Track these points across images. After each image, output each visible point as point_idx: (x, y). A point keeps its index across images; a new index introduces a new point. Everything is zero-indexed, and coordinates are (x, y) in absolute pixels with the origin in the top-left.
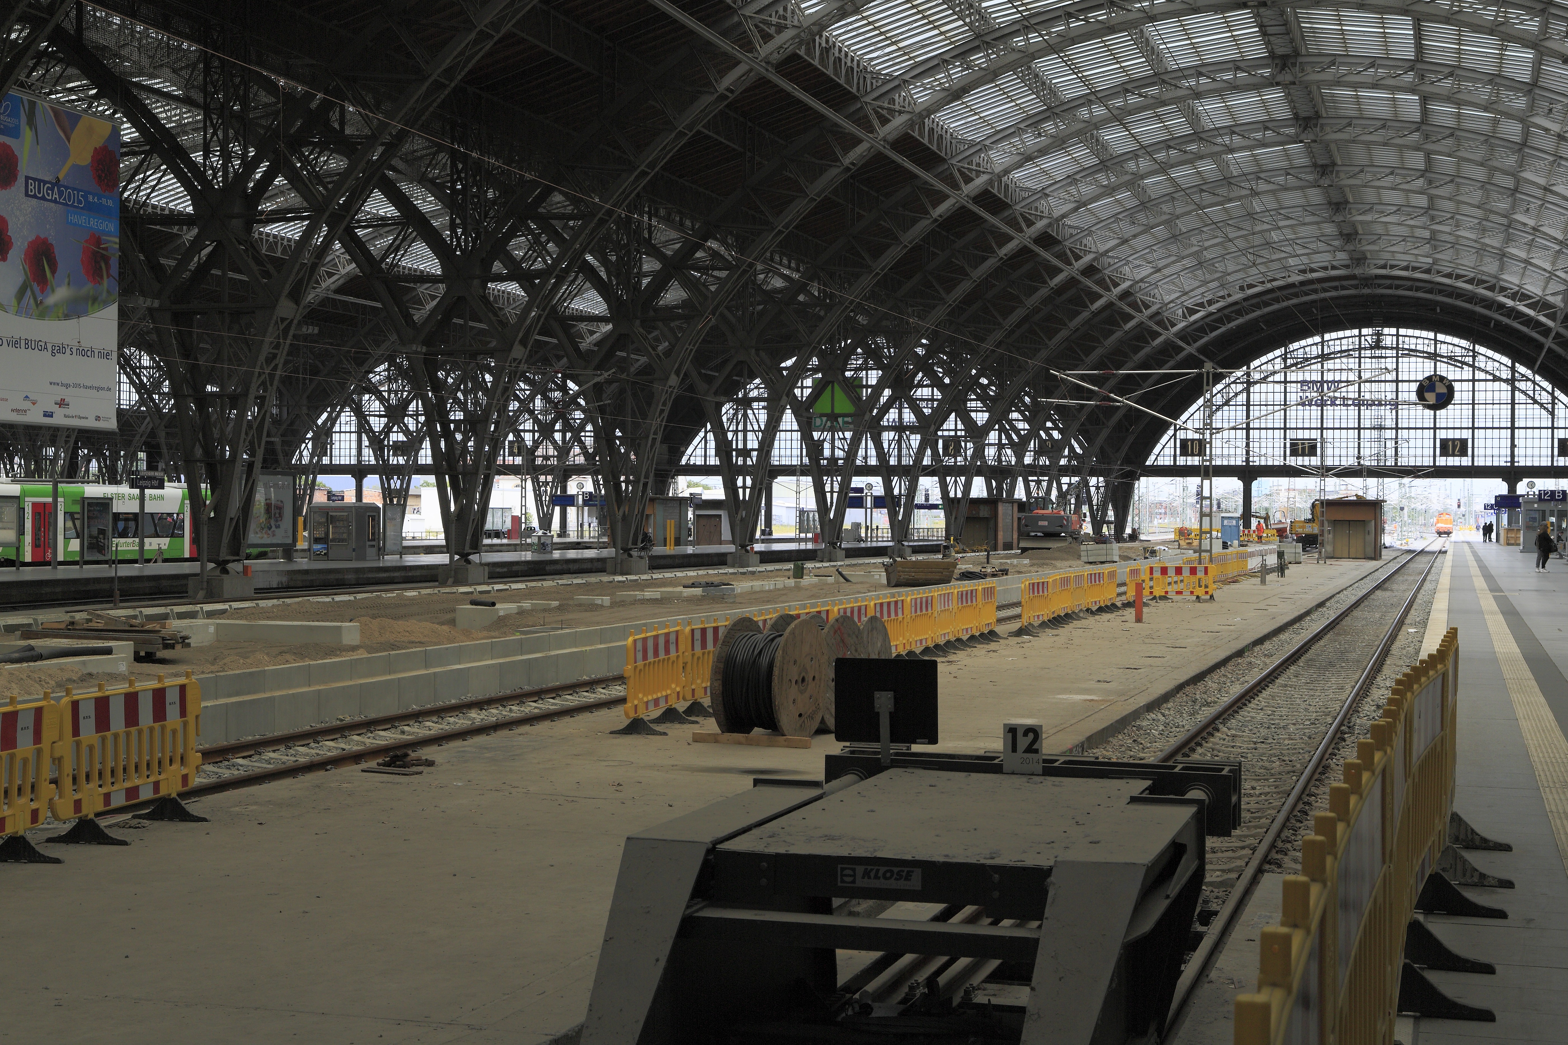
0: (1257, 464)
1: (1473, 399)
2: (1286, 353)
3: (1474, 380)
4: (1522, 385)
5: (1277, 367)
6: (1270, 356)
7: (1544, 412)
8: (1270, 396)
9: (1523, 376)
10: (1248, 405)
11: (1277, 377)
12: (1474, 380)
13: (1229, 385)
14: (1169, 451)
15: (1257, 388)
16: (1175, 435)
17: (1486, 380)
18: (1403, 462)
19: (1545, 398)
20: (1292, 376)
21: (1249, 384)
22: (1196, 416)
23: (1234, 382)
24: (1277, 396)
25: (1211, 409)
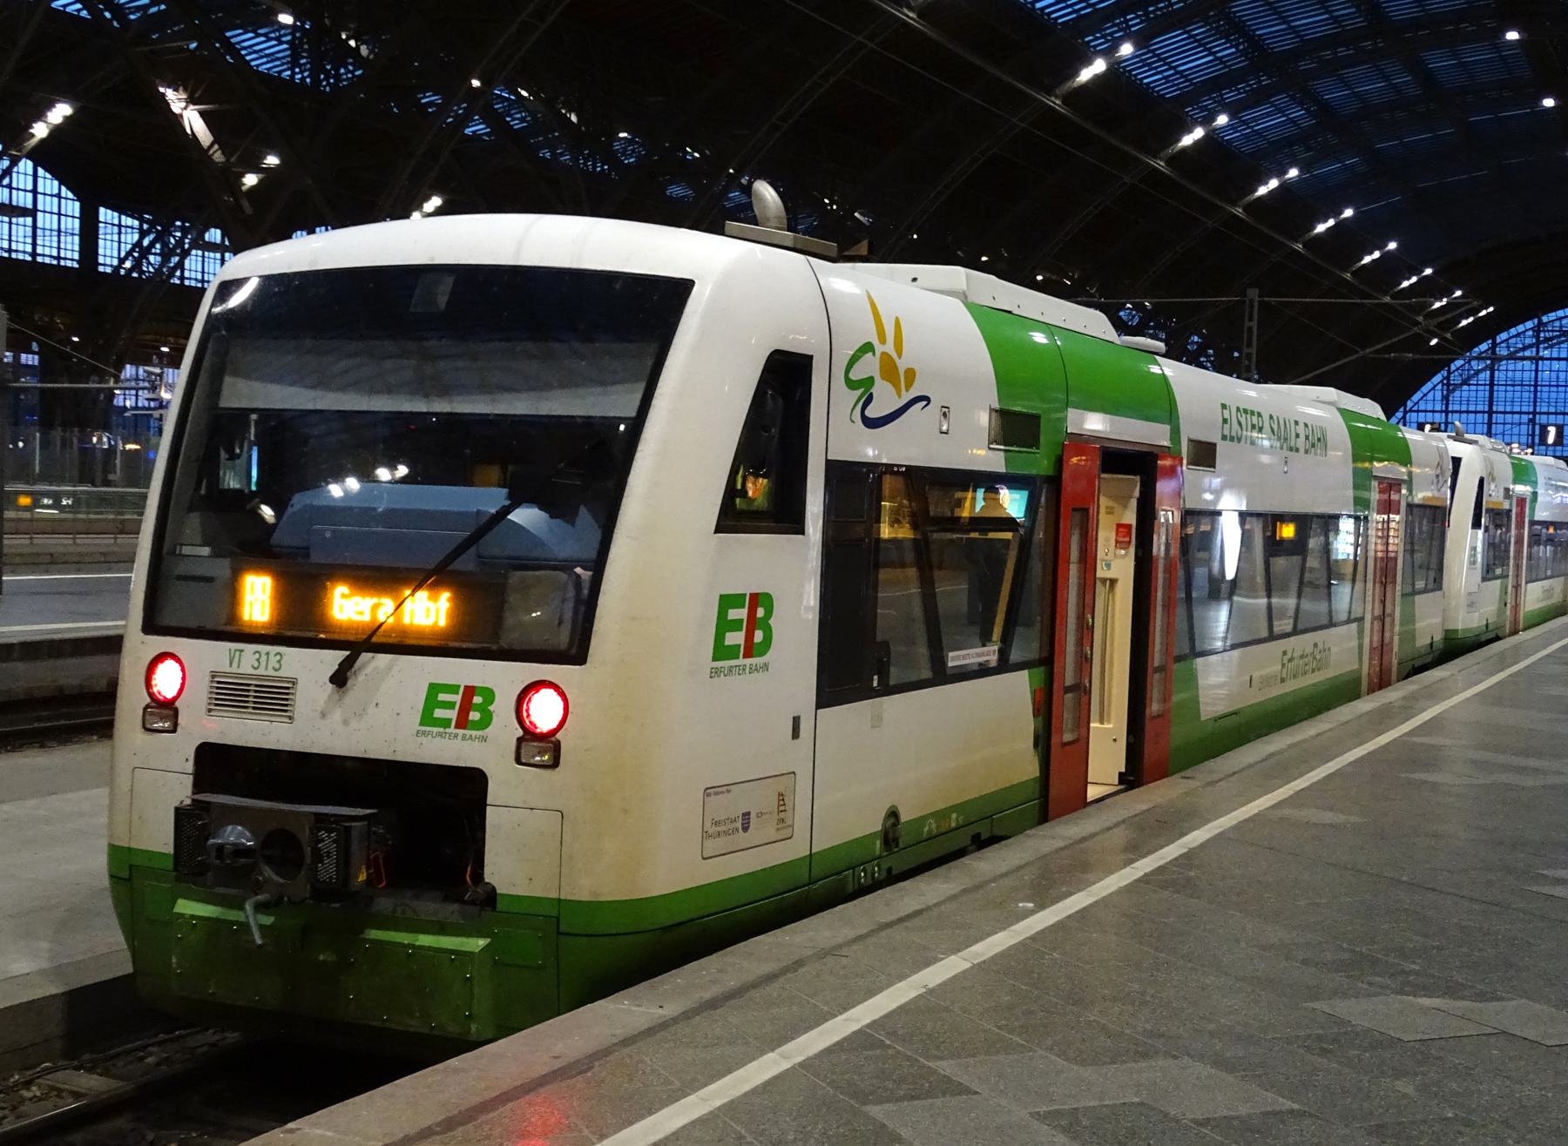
2: (1540, 323)
5: (1528, 341)
6: (1521, 328)
8: (1518, 374)
10: (1492, 385)
11: (1527, 353)
21: (1496, 359)
22: (1430, 396)
24: (1526, 375)
25: (1449, 387)
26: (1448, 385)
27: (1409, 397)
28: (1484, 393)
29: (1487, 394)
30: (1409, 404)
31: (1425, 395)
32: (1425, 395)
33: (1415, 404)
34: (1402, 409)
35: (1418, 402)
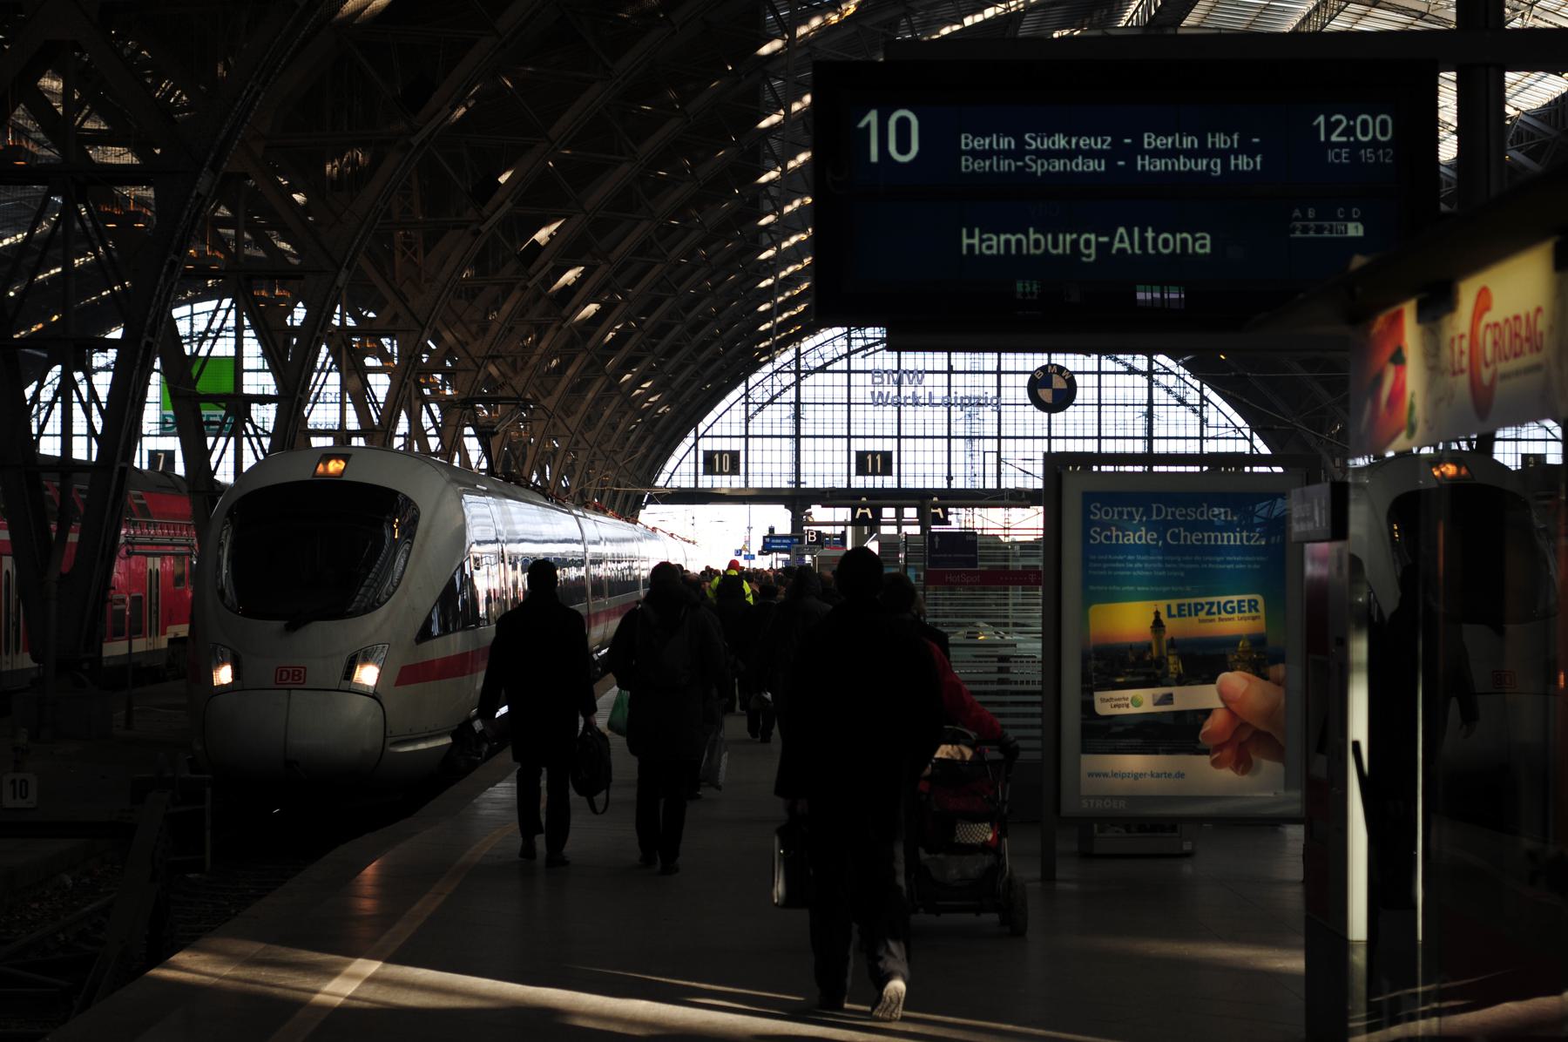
0: (810, 485)
1: (1099, 399)
3: (1099, 373)
4: (1163, 379)
7: (1191, 415)
9: (1166, 368)
12: (1099, 373)
14: (687, 467)
15: (810, 380)
16: (696, 444)
17: (1115, 373)
18: (1008, 483)
19: (1193, 398)
20: (857, 362)
27: (701, 420)
28: (789, 411)
30: (702, 427)
31: (720, 416)
32: (720, 416)
33: (709, 428)
34: (692, 434)
35: (711, 425)
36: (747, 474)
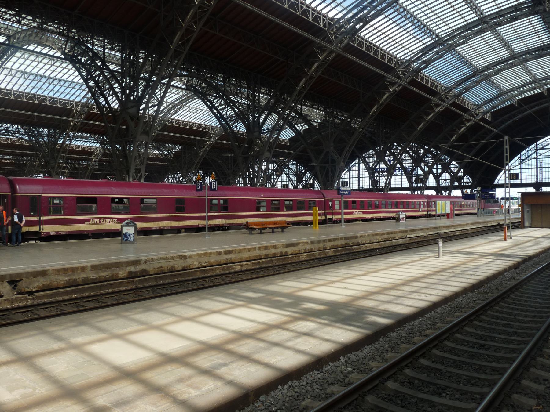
13: (528, 151)
14: (503, 178)
21: (537, 150)
23: (530, 150)
25: (521, 162)
26: (521, 160)
28: (534, 161)
29: (535, 162)
36: (521, 179)
